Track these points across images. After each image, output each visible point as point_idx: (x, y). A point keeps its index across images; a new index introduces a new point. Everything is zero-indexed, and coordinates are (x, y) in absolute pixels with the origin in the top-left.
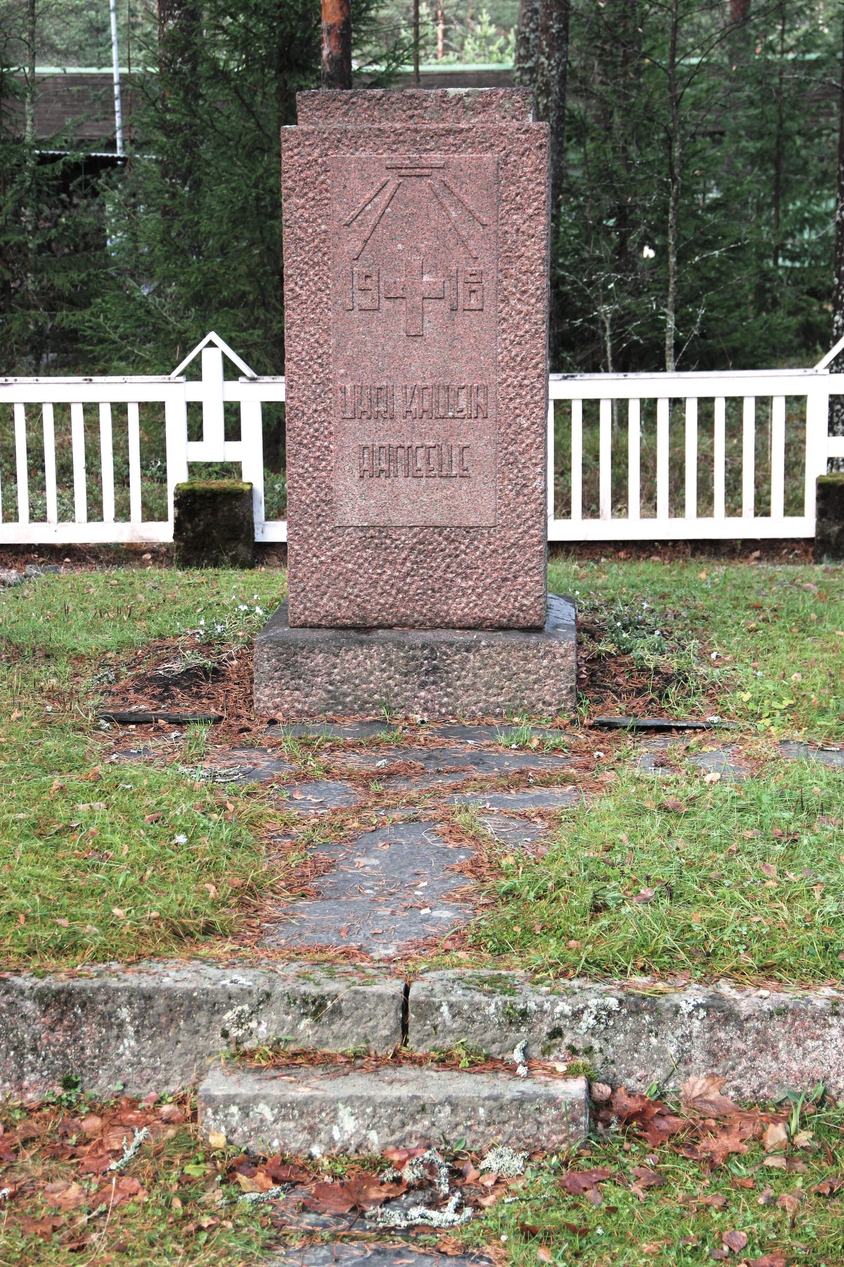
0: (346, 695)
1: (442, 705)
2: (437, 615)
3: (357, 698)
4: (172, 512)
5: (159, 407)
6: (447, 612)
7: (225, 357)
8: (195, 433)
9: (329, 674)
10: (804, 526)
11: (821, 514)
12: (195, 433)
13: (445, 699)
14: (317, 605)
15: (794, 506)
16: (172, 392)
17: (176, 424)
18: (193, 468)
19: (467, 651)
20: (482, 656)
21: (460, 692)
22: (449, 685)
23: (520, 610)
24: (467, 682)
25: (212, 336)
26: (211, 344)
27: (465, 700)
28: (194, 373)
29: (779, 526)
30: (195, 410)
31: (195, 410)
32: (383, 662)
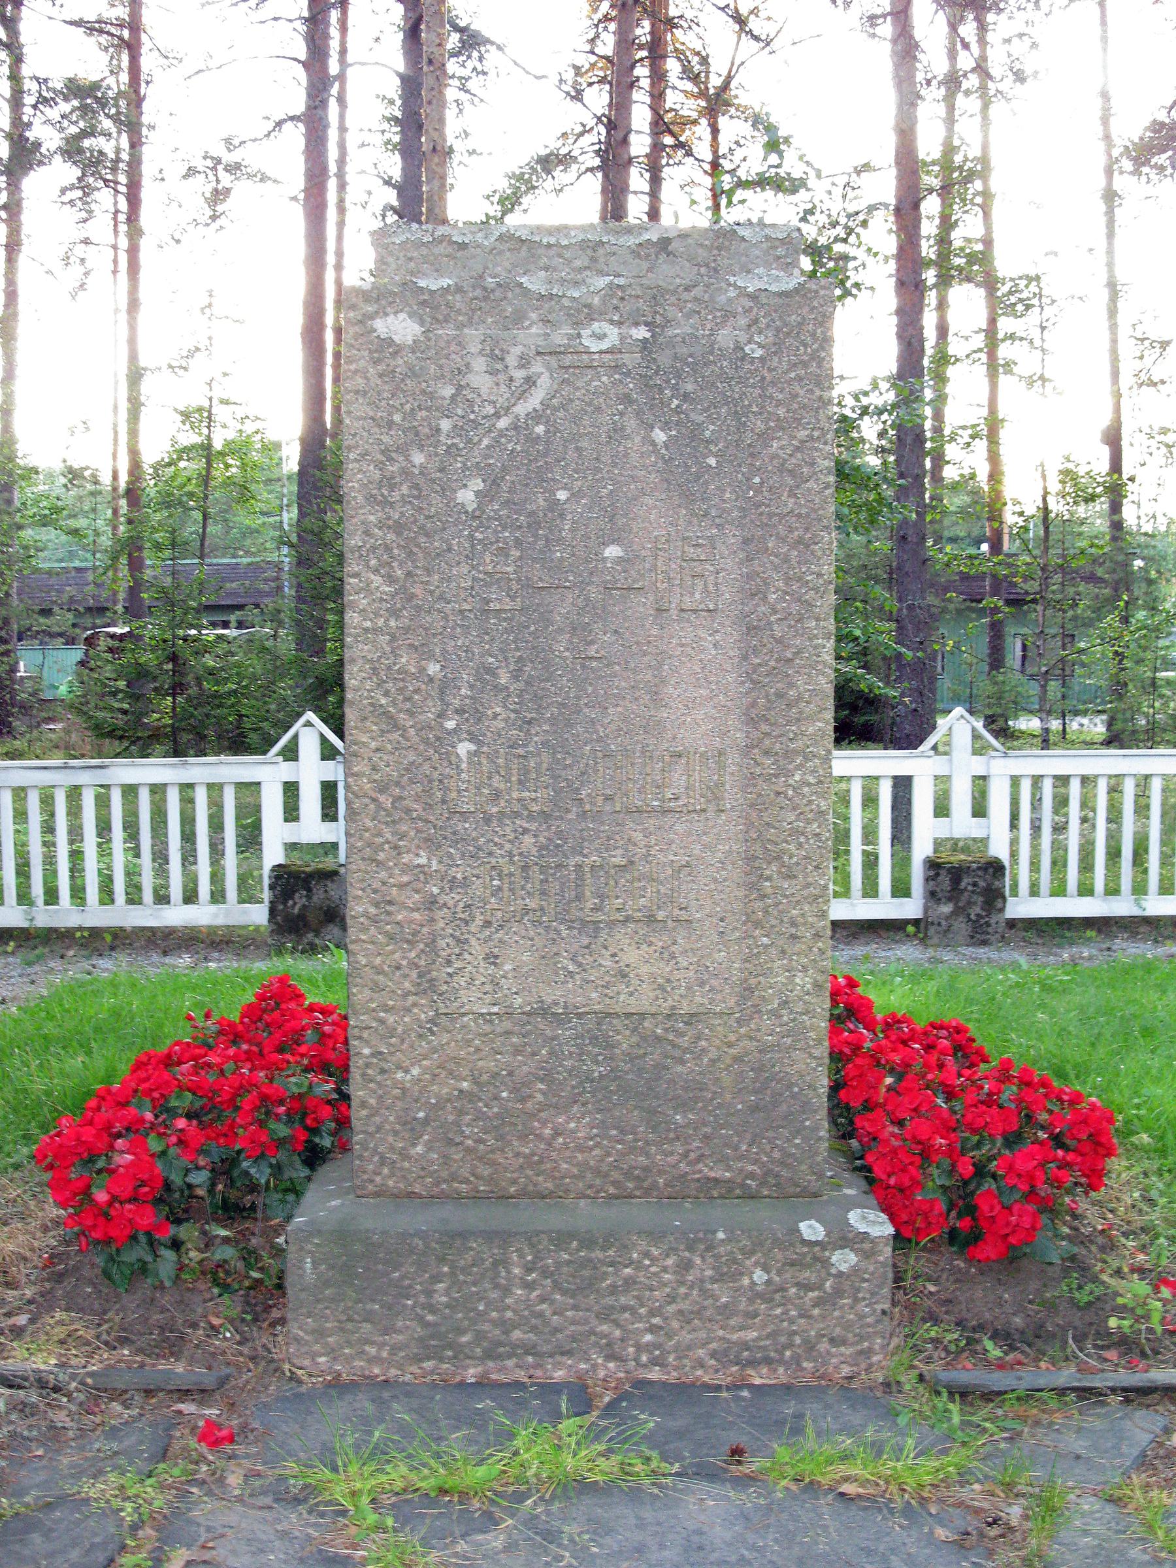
0: (461, 1331)
1: (639, 1348)
2: (628, 1175)
3: (480, 1336)
4: (266, 895)
5: (254, 787)
6: (646, 1169)
7: (324, 739)
8: (291, 812)
9: (429, 1293)
10: (911, 908)
11: (932, 896)
12: (291, 812)
13: (648, 1338)
14: (405, 1156)
15: (901, 889)
16: (268, 773)
17: (272, 803)
18: (291, 847)
19: (690, 1248)
20: (717, 1257)
21: (675, 1324)
22: (652, 1313)
23: (782, 1163)
24: (685, 1306)
25: (310, 716)
26: (308, 724)
27: (686, 1337)
28: (291, 753)
29: (884, 908)
30: (291, 790)
31: (291, 790)
32: (529, 1270)
